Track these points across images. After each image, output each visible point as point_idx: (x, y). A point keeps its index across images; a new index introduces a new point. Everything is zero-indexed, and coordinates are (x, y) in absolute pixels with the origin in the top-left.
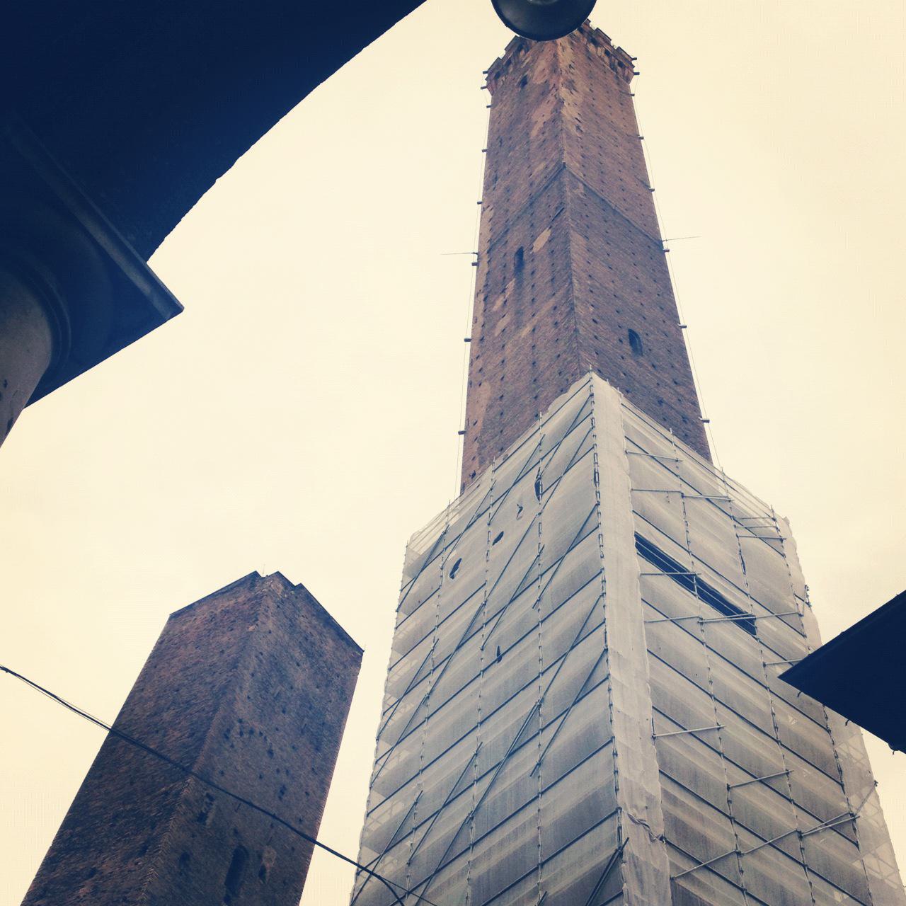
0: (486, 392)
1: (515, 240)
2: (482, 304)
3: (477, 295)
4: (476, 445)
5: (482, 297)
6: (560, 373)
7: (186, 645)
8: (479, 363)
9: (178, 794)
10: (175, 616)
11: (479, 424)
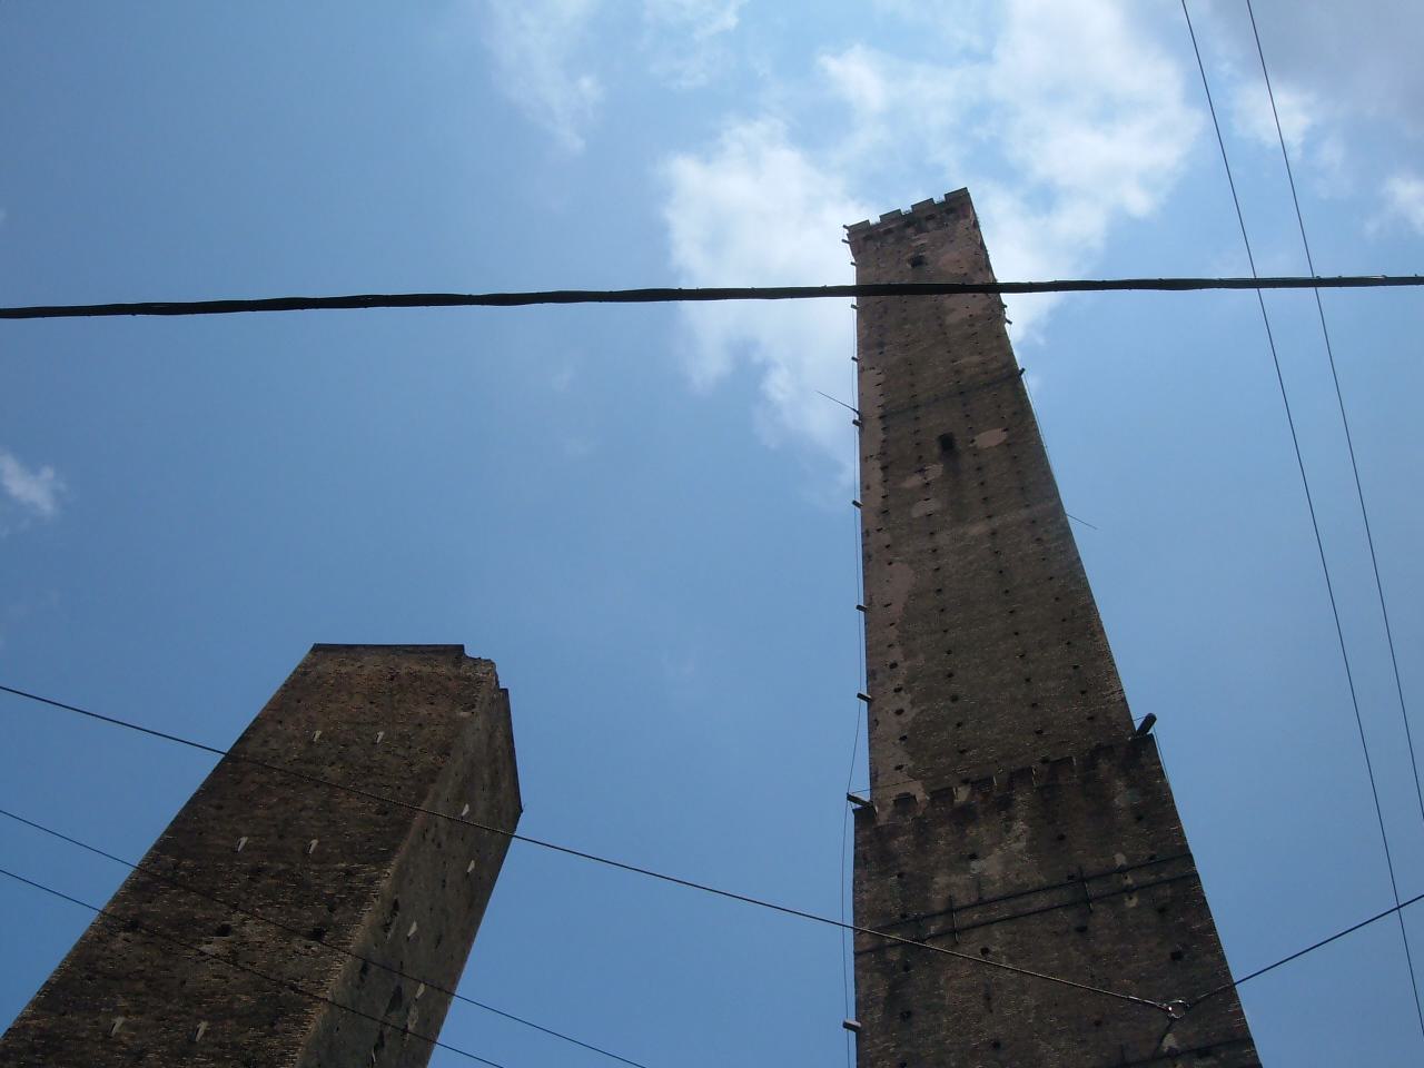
0: (902, 580)
1: (937, 422)
2: (879, 475)
3: (864, 459)
4: (893, 633)
5: (878, 464)
6: (1057, 599)
7: (351, 694)
8: (886, 538)
9: (371, 881)
10: (317, 648)
11: (897, 608)
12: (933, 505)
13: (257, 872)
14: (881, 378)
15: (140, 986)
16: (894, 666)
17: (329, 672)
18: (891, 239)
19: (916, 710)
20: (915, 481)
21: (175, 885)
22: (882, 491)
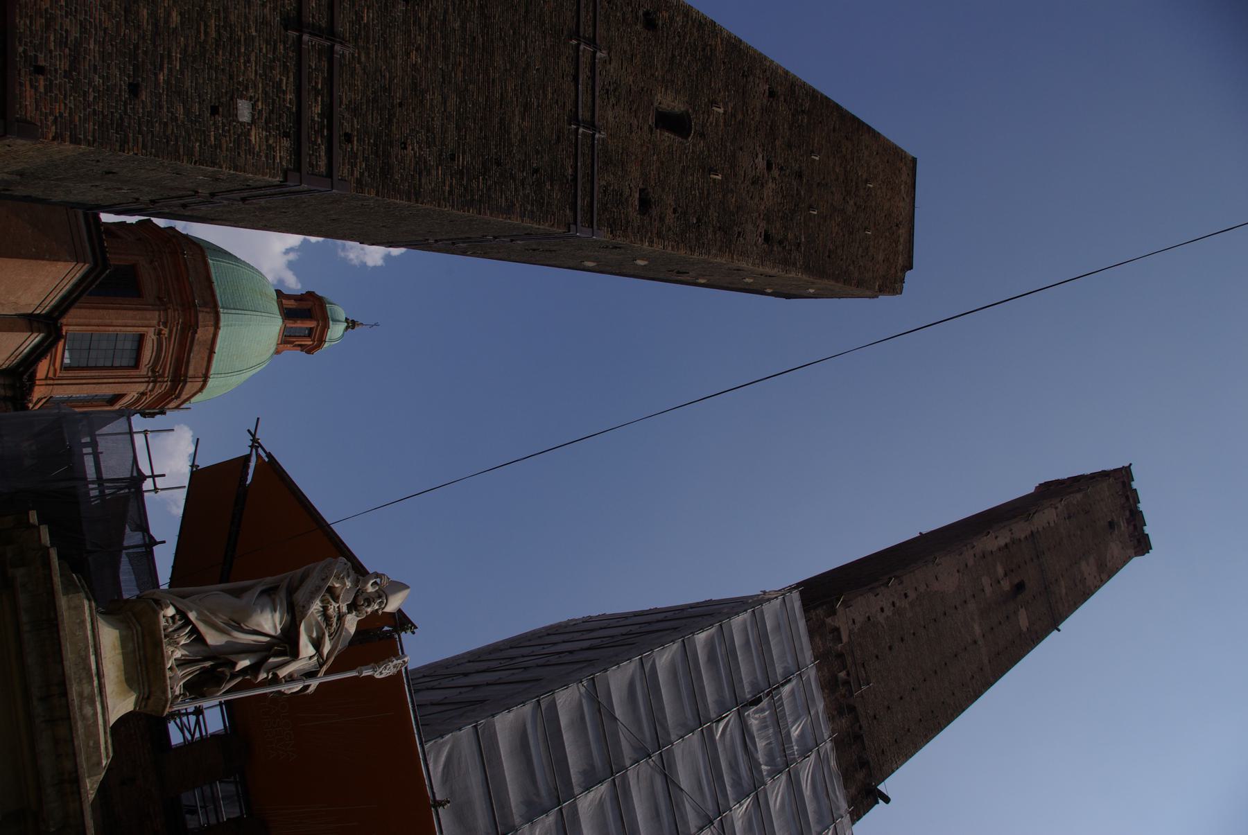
12: (988, 590)
13: (800, 175)
14: (1052, 524)
15: (740, 117)
16: (906, 596)
17: (899, 168)
18: (1123, 500)
19: (882, 621)
20: (1000, 571)
21: (793, 115)
22: (995, 549)
